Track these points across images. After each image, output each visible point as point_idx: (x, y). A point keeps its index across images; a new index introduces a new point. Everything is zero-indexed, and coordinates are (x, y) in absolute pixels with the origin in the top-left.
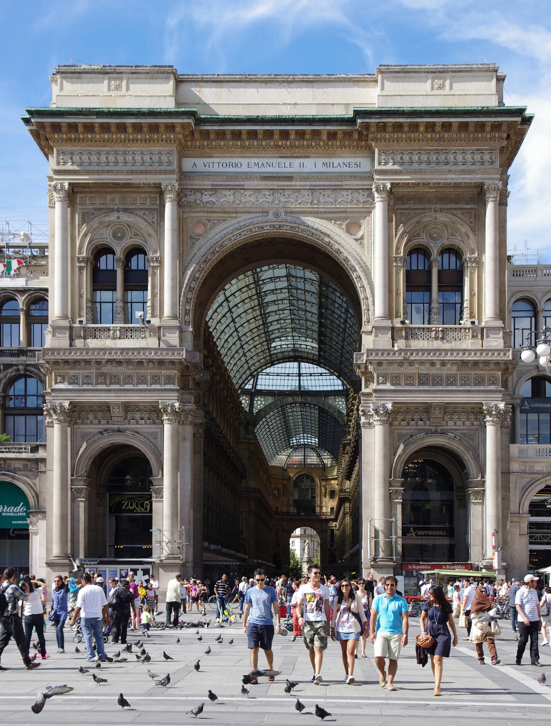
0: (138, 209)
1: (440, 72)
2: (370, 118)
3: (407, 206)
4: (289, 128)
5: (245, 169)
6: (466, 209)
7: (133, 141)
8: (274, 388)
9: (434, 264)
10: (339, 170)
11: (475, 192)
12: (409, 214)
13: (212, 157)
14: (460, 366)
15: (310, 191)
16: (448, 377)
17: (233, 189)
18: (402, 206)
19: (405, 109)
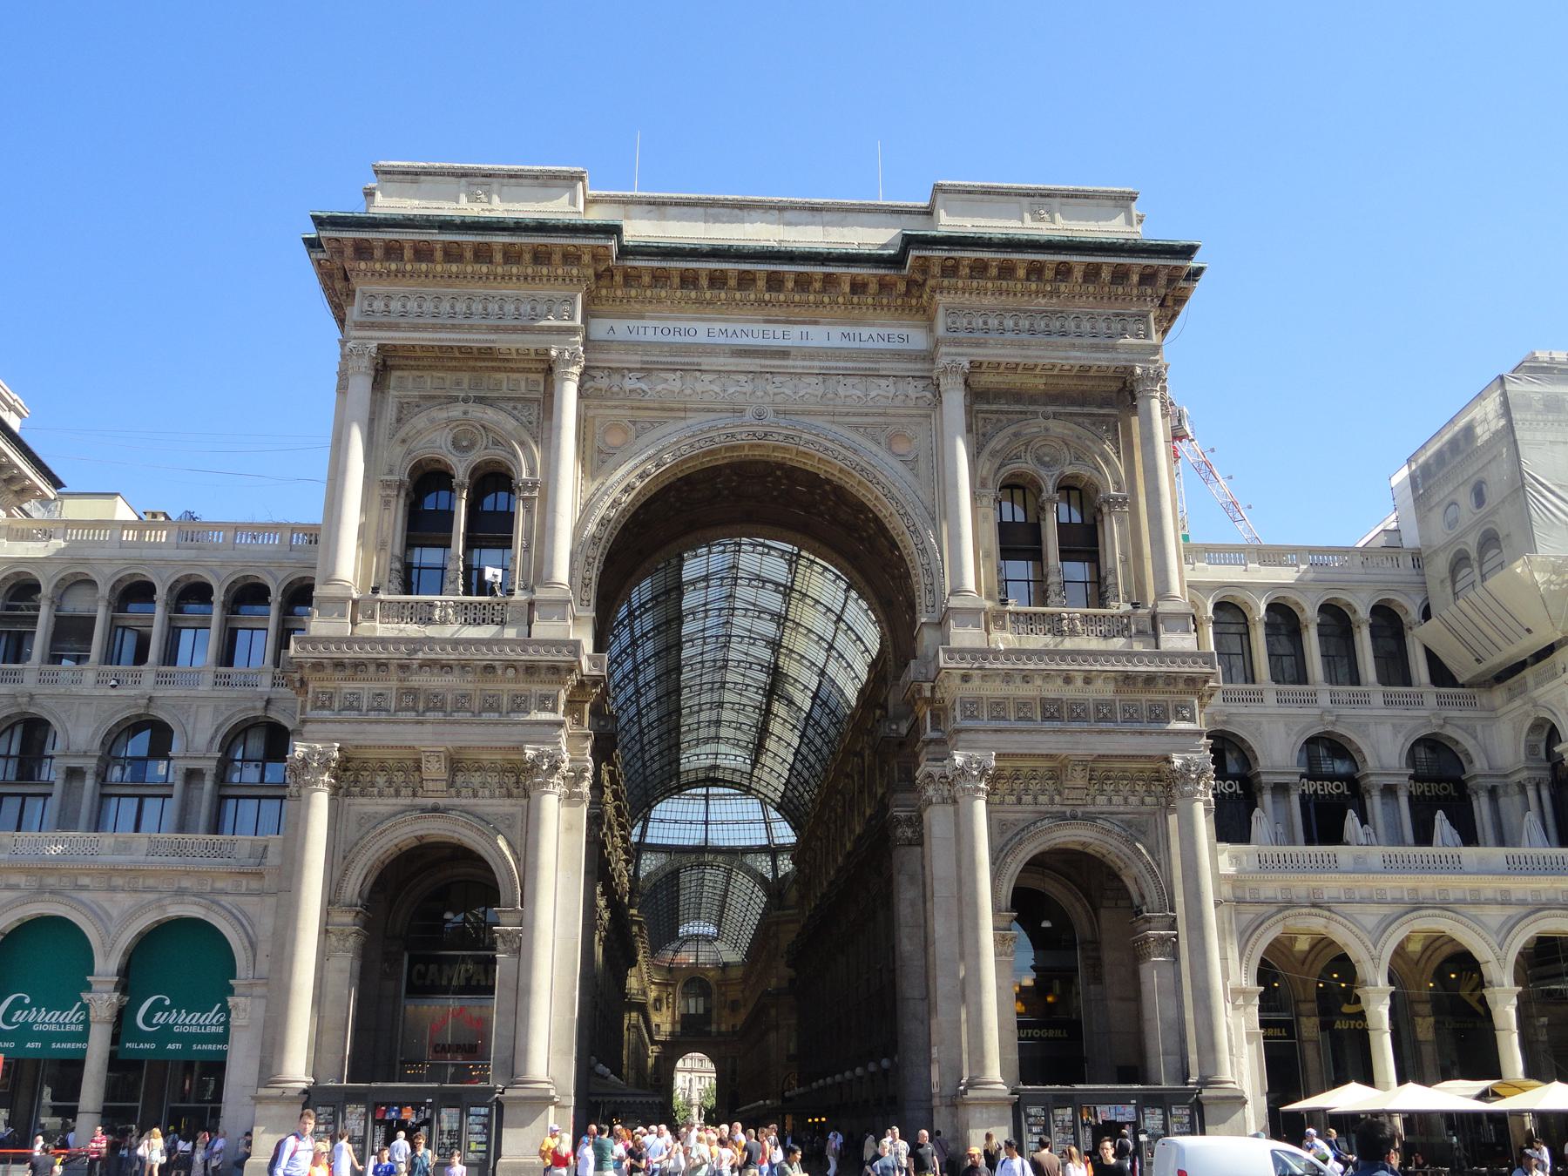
0: (503, 398)
1: (1042, 196)
2: (933, 250)
3: (994, 407)
4: (786, 268)
5: (702, 338)
6: (1099, 415)
7: (503, 277)
8: (670, 842)
9: (1048, 507)
10: (870, 345)
11: (1115, 389)
12: (999, 420)
13: (642, 318)
14: (1120, 684)
15: (820, 377)
16: (1099, 705)
17: (681, 370)
18: (986, 407)
19: (992, 236)
